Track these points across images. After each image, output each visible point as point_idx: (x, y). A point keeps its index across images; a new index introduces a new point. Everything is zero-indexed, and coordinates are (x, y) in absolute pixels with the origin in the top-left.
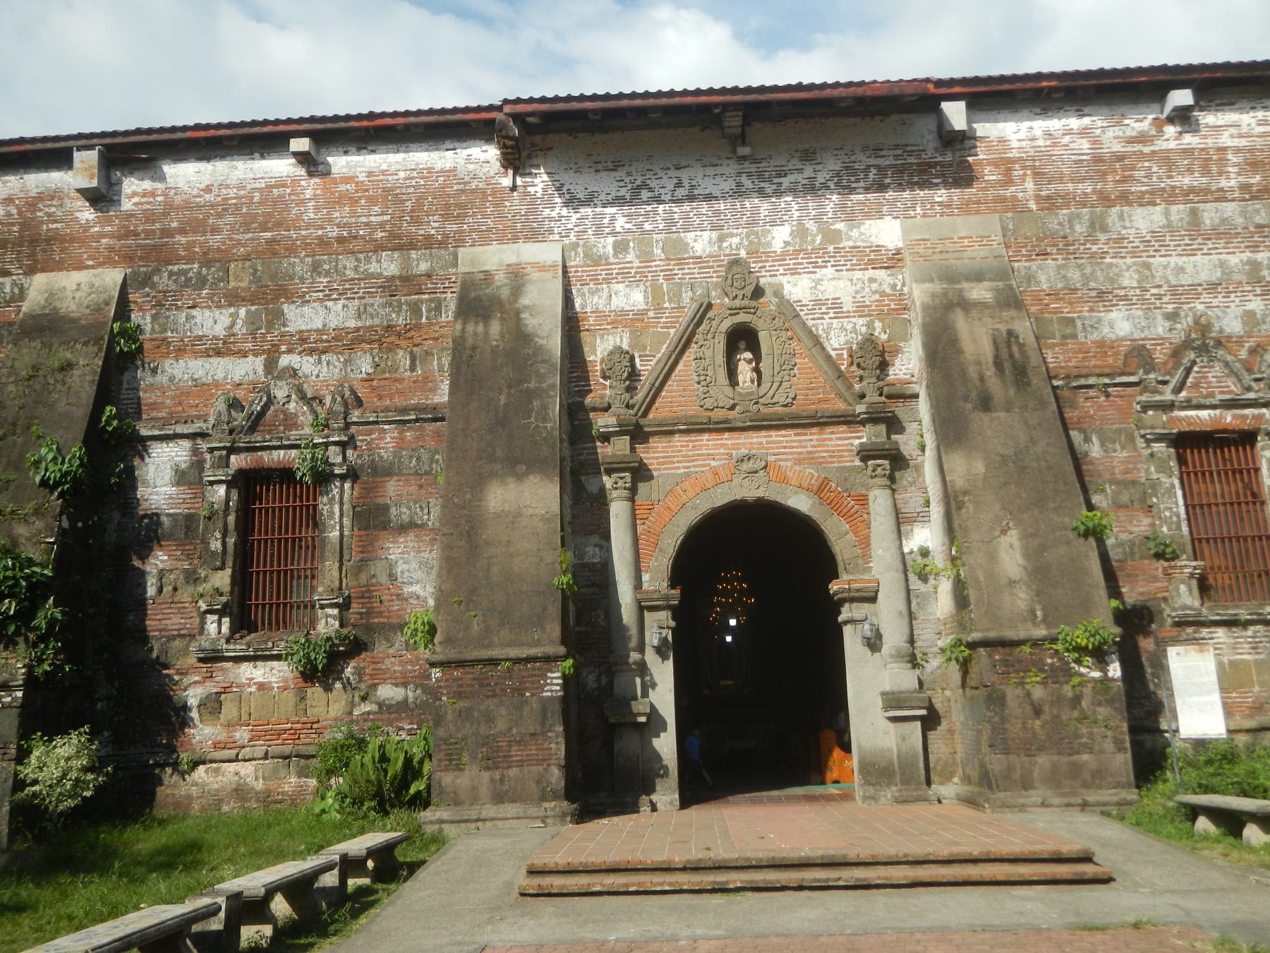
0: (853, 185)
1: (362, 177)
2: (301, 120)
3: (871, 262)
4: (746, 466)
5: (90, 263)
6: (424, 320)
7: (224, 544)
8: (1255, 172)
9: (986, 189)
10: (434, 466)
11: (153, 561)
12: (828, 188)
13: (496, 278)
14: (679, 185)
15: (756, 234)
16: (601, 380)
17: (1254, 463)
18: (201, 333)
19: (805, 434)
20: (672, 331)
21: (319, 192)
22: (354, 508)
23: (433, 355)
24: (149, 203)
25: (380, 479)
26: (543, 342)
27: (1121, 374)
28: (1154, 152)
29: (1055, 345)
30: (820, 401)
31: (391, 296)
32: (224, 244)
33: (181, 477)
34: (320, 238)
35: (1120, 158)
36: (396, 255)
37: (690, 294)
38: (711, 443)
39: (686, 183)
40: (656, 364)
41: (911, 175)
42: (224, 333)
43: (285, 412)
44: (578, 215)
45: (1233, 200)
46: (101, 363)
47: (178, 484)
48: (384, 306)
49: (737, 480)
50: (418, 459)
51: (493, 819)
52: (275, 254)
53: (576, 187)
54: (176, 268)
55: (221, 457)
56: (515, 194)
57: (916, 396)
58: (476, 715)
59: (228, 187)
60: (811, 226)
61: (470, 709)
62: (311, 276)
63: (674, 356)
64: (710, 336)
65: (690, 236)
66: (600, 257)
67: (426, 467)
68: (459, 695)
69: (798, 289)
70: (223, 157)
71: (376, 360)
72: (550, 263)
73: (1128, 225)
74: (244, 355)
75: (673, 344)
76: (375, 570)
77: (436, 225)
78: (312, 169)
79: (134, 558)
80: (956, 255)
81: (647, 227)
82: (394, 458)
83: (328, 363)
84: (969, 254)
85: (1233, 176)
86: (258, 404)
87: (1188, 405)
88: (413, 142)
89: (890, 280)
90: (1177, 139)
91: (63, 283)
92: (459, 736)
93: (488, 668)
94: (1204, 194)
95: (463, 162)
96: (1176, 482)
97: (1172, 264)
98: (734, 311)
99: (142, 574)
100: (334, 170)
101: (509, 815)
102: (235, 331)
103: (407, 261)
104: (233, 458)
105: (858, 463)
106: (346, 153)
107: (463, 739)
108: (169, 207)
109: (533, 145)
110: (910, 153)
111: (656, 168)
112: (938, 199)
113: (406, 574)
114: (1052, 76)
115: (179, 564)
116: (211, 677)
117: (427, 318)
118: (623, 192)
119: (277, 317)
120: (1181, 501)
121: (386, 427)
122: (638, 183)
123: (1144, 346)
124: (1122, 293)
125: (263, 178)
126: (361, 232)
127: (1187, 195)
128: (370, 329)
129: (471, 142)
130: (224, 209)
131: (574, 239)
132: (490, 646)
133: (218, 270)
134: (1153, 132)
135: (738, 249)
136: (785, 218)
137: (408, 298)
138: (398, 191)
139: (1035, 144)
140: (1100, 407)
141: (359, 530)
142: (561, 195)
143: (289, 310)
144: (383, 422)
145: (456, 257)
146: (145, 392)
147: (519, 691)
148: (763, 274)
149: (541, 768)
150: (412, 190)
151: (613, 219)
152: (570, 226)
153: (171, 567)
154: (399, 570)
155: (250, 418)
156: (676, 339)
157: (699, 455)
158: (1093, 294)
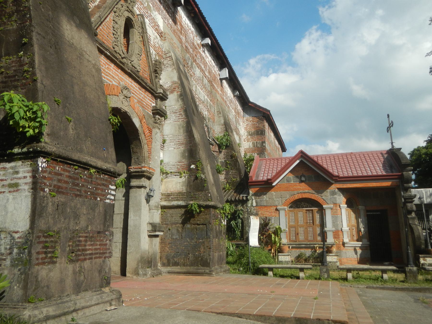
4: (125, 92)
19: (141, 90)
35: (196, 48)
38: (114, 70)
51: (83, 308)
58: (69, 210)
61: (64, 204)
63: (109, 11)
68: (58, 190)
92: (56, 229)
93: (80, 170)
101: (93, 303)
107: (58, 233)
132: (81, 151)
147: (94, 195)
149: (101, 260)
157: (109, 74)
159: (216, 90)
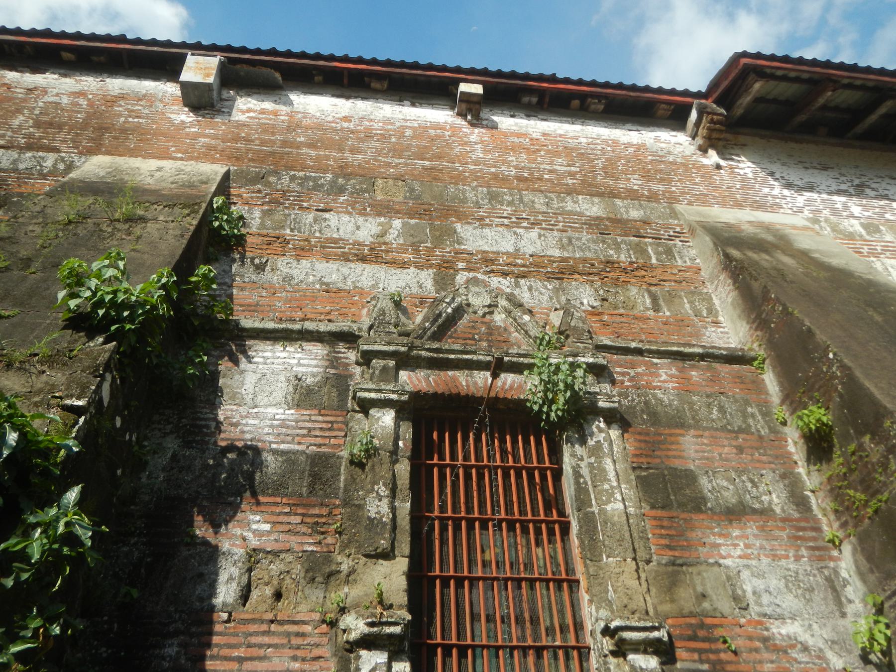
1: (534, 136)
2: (472, 71)
5: (180, 155)
6: (654, 261)
7: (393, 509)
10: (751, 421)
11: (238, 531)
18: (335, 236)
22: (634, 469)
23: (680, 297)
25: (667, 431)
26: (871, 277)
31: (600, 233)
32: (368, 162)
36: (596, 200)
42: (372, 240)
43: (488, 325)
44: (805, 198)
46: (195, 222)
47: (298, 406)
50: (721, 409)
53: (789, 176)
54: (301, 174)
55: (385, 369)
62: (490, 202)
67: (738, 422)
70: (364, 98)
71: (601, 292)
74: (404, 265)
76: (703, 584)
77: (639, 182)
79: (199, 519)
82: (681, 400)
83: (530, 289)
86: (449, 304)
88: (591, 119)
91: (137, 165)
95: (652, 141)
99: (212, 554)
100: (500, 126)
102: (387, 241)
104: (404, 375)
106: (512, 116)
108: (293, 126)
113: (765, 599)
115: (294, 542)
117: (657, 260)
118: (843, 187)
119: (445, 234)
121: (655, 360)
122: (857, 182)
125: (415, 120)
126: (546, 176)
128: (584, 260)
129: (656, 129)
131: (811, 215)
137: (626, 238)
138: (583, 151)
141: (653, 507)
142: (776, 180)
144: (650, 352)
146: (243, 289)
150: (599, 152)
151: (846, 207)
153: (277, 547)
154: (748, 588)
155: (435, 320)
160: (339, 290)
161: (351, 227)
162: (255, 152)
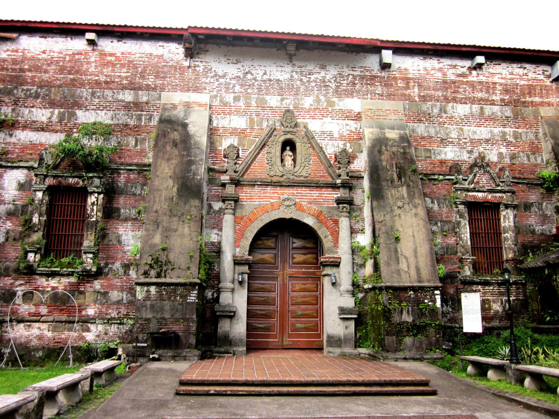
0: (342, 82)
1: (119, 54)
2: (92, 25)
3: (347, 117)
4: (287, 203)
6: (143, 124)
7: (39, 220)
8: (507, 94)
9: (398, 90)
12: (331, 82)
13: (178, 107)
14: (265, 74)
15: (298, 99)
16: (223, 159)
17: (498, 217)
20: (257, 139)
21: (98, 59)
24: (14, 55)
27: (448, 175)
28: (467, 81)
29: (422, 160)
30: (321, 176)
32: (50, 78)
33: (21, 187)
34: (96, 81)
35: (454, 82)
36: (132, 92)
37: (266, 123)
39: (268, 73)
40: (249, 154)
41: (367, 80)
44: (218, 83)
45: (497, 105)
48: (124, 115)
49: (282, 208)
52: (74, 86)
54: (25, 88)
56: (190, 70)
57: (363, 178)
59: (54, 52)
60: (322, 98)
63: (257, 151)
64: (274, 143)
65: (268, 98)
66: (227, 103)
69: (315, 126)
72: (204, 103)
73: (455, 111)
75: (257, 146)
77: (152, 80)
78: (95, 48)
80: (384, 117)
81: (249, 91)
84: (389, 117)
85: (498, 95)
87: (474, 190)
89: (355, 126)
90: (477, 77)
94: (486, 101)
96: (467, 223)
97: (472, 130)
98: (286, 133)
103: (137, 95)
105: (335, 205)
109: (200, 48)
110: (367, 71)
111: (255, 65)
112: (377, 92)
114: (429, 44)
116: (29, 282)
117: (145, 123)
118: (239, 74)
120: (468, 231)
122: (247, 71)
123: (458, 164)
124: (451, 140)
126: (116, 80)
127: (480, 101)
130: (51, 62)
133: (46, 90)
134: (468, 73)
135: (289, 105)
136: (311, 93)
138: (135, 63)
139: (420, 72)
140: (439, 189)
143: (79, 113)
145: (160, 97)
148: (300, 117)
150: (141, 63)
151: (234, 86)
152: (214, 87)
156: (259, 143)
158: (439, 139)
159: (542, 104)
160: (35, 144)
161: (41, 115)
162: (10, 76)
